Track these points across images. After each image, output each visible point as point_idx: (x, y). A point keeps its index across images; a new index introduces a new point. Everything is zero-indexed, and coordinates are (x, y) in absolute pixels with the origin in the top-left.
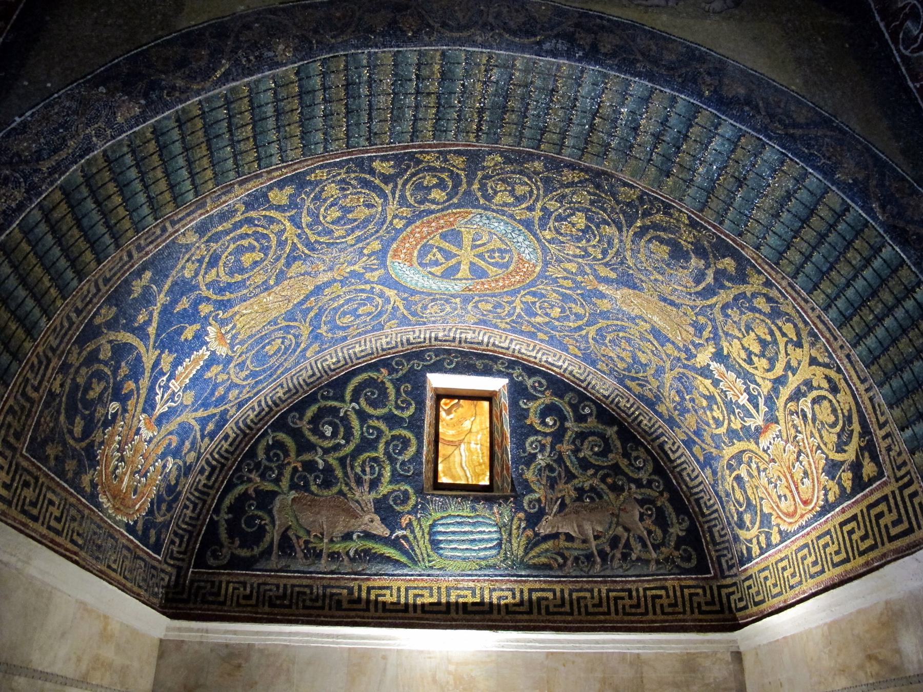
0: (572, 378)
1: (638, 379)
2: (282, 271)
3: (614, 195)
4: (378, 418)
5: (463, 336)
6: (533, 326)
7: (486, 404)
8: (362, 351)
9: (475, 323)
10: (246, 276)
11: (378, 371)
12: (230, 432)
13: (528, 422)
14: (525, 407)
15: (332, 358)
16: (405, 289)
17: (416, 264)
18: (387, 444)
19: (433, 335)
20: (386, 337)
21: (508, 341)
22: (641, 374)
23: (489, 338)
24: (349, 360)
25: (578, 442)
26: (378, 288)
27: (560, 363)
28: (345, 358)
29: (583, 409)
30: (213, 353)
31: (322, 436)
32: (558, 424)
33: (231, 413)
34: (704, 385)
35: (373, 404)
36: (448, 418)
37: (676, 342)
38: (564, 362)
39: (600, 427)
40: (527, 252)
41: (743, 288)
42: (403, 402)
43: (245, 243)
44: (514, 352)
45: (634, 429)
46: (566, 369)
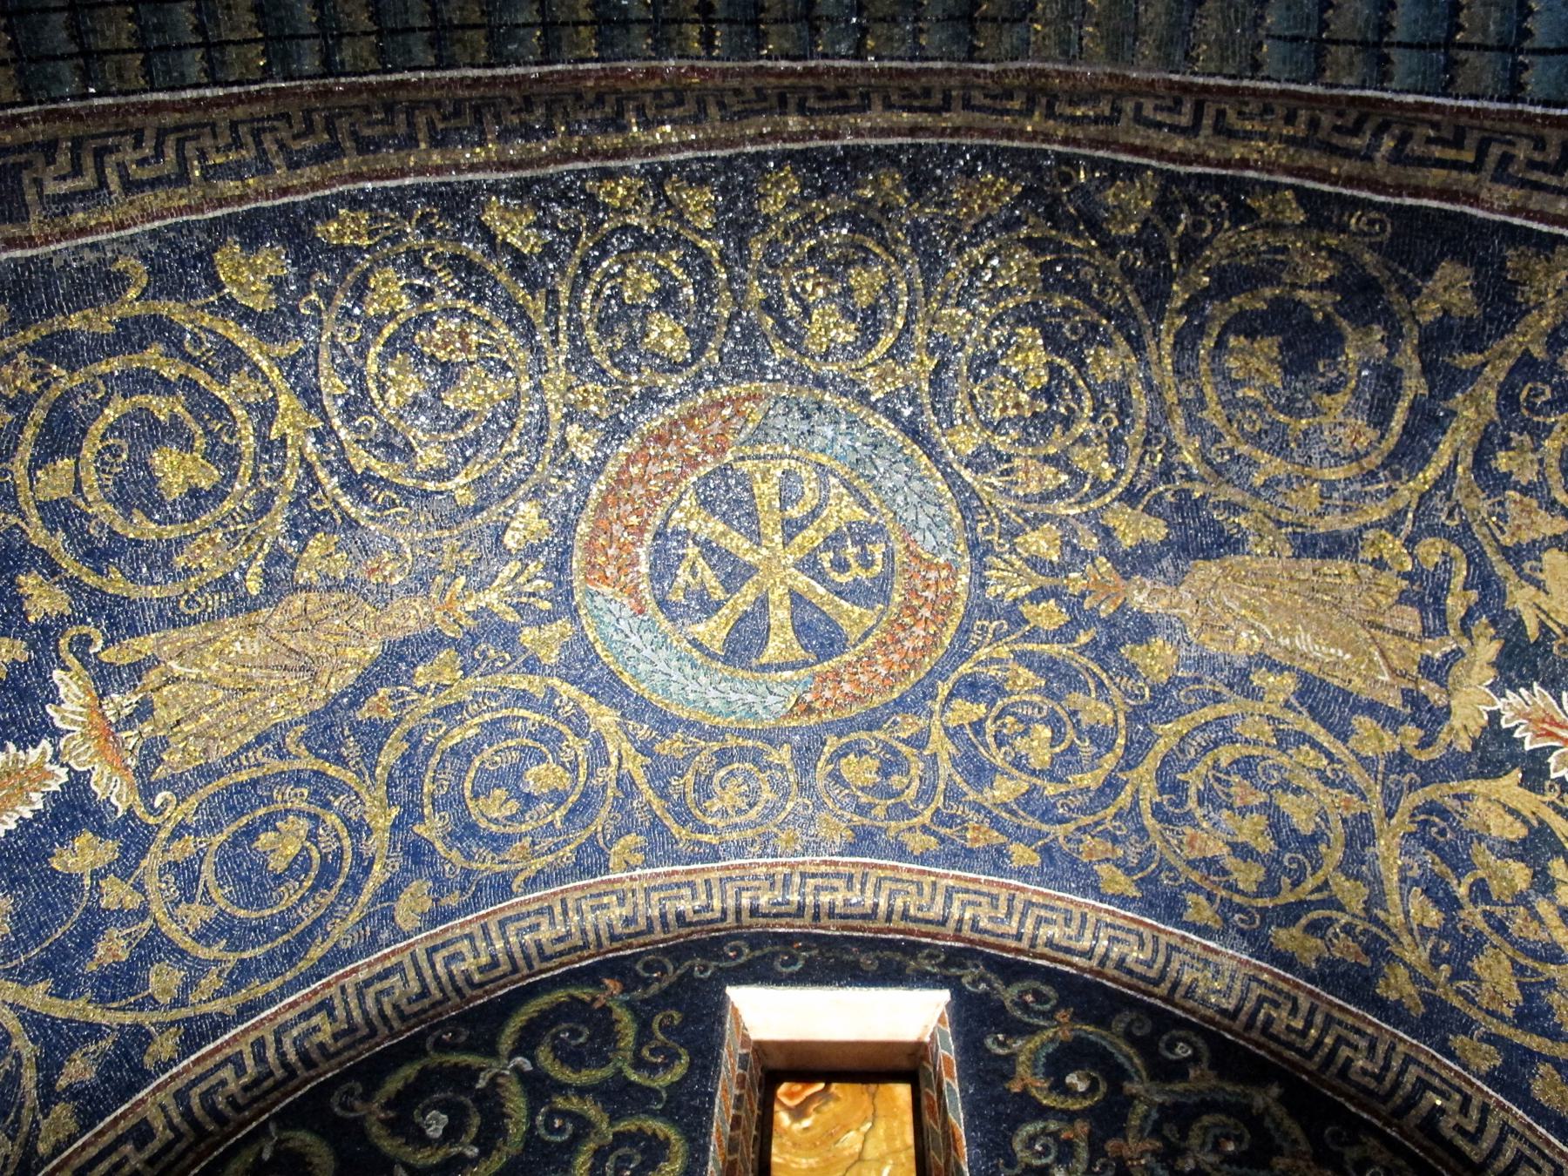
0: (1126, 978)
1: (1302, 906)
2: (277, 557)
3: (1095, 227)
4: (581, 1091)
5: (825, 898)
6: (996, 823)
7: (902, 1092)
8: (560, 939)
9: (852, 849)
10: (172, 532)
11: (597, 984)
12: (159, 1124)
13: (1016, 1088)
14: (1001, 1051)
15: (476, 946)
16: (639, 709)
17: (652, 607)
18: (600, 1155)
19: (745, 902)
20: (621, 901)
21: (940, 900)
22: (1310, 883)
23: (892, 894)
24: (521, 963)
25: (1170, 1130)
26: (567, 690)
27: (1086, 944)
28: (511, 957)
29: (1171, 1047)
30: (78, 781)
31: (421, 1139)
32: (1103, 1088)
33: (165, 1046)
34: (1497, 807)
35: (574, 1059)
36: (797, 1127)
37: (1379, 695)
38: (1096, 938)
39: (1229, 1088)
40: (924, 522)
41: (1516, 342)
42: (653, 1052)
43: (162, 407)
44: (959, 930)
45: (1332, 1088)
46: (1106, 956)
